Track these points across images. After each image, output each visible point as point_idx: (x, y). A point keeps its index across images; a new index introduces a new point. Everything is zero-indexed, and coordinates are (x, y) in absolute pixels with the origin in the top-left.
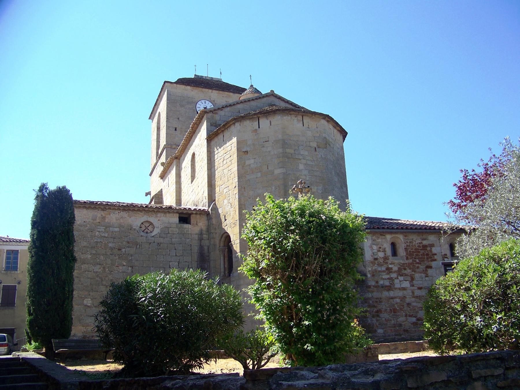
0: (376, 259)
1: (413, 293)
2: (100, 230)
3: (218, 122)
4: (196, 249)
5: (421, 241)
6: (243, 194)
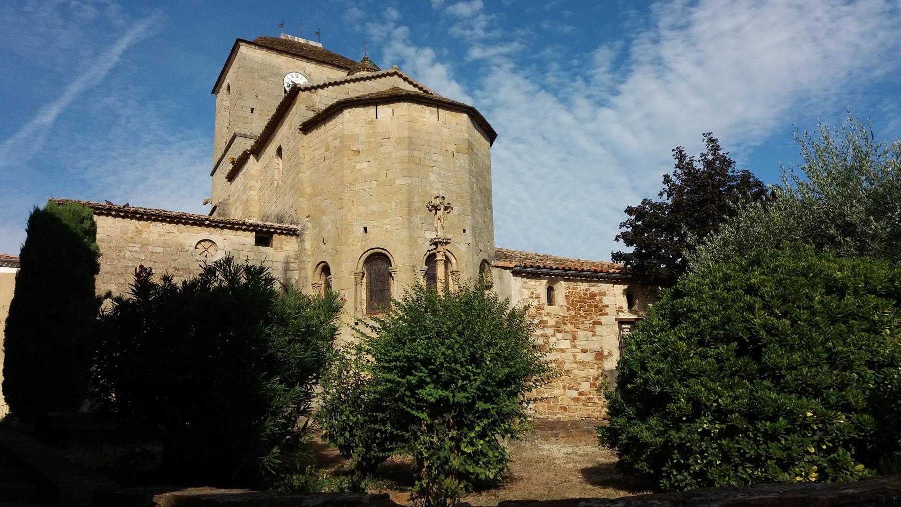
1: (575, 356)
2: (134, 249)
3: (317, 104)
6: (351, 209)
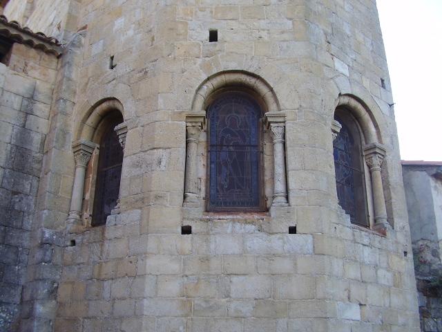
4: (9, 133)
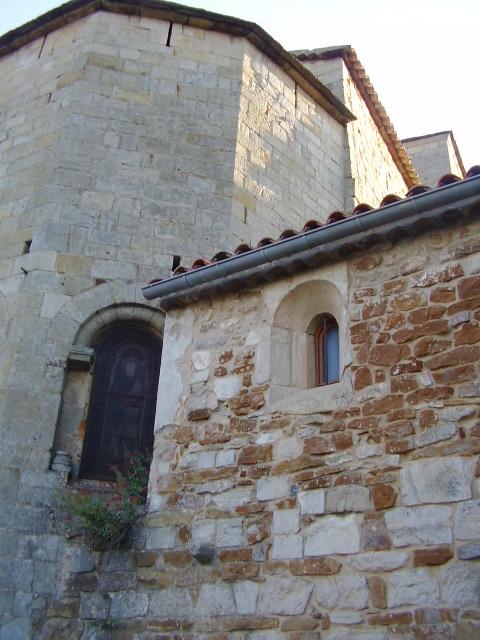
0: (199, 416)
1: (378, 590)
5: (454, 264)
